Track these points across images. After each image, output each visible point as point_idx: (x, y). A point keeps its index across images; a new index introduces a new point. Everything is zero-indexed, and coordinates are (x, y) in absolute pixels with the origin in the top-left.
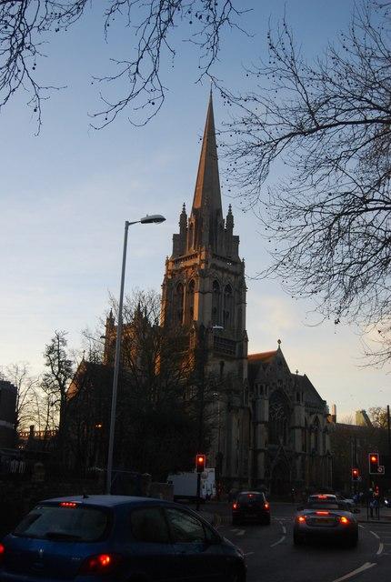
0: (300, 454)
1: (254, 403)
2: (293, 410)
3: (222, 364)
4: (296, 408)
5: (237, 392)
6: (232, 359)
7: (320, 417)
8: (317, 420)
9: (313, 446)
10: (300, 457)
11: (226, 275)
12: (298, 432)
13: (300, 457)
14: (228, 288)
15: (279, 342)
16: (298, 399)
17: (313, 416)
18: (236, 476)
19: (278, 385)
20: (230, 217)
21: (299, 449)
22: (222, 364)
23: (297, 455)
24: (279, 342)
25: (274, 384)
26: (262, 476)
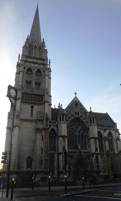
0: (94, 153)
1: (57, 126)
2: (88, 129)
3: (32, 107)
4: (90, 127)
5: (41, 121)
6: (39, 104)
7: (113, 132)
8: (110, 133)
9: (107, 148)
10: (95, 156)
11: (36, 65)
12: (92, 141)
13: (95, 156)
14: (39, 71)
15: (76, 93)
16: (91, 123)
17: (107, 132)
18: (40, 170)
19: (77, 116)
20: (44, 42)
21: (93, 151)
22: (32, 107)
23: (93, 154)
24: (76, 93)
25: (73, 115)
26: (61, 169)
